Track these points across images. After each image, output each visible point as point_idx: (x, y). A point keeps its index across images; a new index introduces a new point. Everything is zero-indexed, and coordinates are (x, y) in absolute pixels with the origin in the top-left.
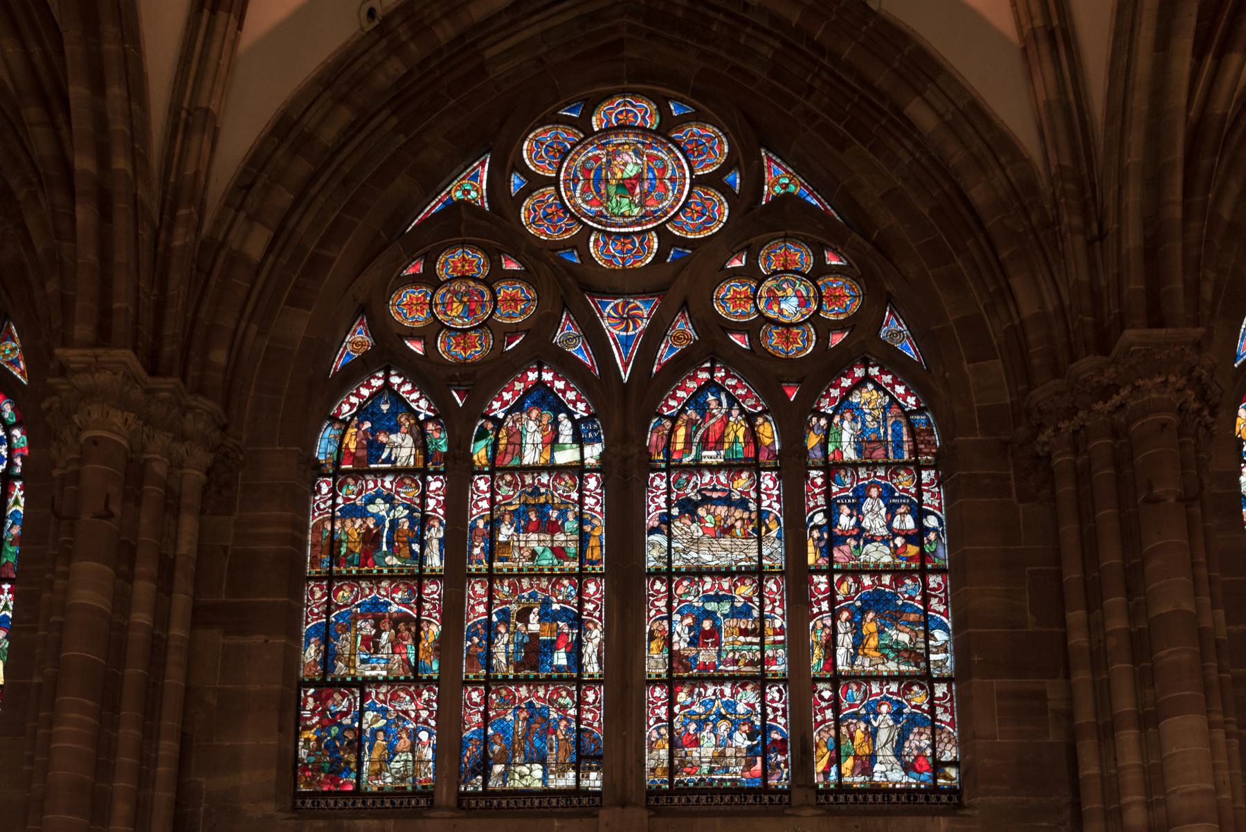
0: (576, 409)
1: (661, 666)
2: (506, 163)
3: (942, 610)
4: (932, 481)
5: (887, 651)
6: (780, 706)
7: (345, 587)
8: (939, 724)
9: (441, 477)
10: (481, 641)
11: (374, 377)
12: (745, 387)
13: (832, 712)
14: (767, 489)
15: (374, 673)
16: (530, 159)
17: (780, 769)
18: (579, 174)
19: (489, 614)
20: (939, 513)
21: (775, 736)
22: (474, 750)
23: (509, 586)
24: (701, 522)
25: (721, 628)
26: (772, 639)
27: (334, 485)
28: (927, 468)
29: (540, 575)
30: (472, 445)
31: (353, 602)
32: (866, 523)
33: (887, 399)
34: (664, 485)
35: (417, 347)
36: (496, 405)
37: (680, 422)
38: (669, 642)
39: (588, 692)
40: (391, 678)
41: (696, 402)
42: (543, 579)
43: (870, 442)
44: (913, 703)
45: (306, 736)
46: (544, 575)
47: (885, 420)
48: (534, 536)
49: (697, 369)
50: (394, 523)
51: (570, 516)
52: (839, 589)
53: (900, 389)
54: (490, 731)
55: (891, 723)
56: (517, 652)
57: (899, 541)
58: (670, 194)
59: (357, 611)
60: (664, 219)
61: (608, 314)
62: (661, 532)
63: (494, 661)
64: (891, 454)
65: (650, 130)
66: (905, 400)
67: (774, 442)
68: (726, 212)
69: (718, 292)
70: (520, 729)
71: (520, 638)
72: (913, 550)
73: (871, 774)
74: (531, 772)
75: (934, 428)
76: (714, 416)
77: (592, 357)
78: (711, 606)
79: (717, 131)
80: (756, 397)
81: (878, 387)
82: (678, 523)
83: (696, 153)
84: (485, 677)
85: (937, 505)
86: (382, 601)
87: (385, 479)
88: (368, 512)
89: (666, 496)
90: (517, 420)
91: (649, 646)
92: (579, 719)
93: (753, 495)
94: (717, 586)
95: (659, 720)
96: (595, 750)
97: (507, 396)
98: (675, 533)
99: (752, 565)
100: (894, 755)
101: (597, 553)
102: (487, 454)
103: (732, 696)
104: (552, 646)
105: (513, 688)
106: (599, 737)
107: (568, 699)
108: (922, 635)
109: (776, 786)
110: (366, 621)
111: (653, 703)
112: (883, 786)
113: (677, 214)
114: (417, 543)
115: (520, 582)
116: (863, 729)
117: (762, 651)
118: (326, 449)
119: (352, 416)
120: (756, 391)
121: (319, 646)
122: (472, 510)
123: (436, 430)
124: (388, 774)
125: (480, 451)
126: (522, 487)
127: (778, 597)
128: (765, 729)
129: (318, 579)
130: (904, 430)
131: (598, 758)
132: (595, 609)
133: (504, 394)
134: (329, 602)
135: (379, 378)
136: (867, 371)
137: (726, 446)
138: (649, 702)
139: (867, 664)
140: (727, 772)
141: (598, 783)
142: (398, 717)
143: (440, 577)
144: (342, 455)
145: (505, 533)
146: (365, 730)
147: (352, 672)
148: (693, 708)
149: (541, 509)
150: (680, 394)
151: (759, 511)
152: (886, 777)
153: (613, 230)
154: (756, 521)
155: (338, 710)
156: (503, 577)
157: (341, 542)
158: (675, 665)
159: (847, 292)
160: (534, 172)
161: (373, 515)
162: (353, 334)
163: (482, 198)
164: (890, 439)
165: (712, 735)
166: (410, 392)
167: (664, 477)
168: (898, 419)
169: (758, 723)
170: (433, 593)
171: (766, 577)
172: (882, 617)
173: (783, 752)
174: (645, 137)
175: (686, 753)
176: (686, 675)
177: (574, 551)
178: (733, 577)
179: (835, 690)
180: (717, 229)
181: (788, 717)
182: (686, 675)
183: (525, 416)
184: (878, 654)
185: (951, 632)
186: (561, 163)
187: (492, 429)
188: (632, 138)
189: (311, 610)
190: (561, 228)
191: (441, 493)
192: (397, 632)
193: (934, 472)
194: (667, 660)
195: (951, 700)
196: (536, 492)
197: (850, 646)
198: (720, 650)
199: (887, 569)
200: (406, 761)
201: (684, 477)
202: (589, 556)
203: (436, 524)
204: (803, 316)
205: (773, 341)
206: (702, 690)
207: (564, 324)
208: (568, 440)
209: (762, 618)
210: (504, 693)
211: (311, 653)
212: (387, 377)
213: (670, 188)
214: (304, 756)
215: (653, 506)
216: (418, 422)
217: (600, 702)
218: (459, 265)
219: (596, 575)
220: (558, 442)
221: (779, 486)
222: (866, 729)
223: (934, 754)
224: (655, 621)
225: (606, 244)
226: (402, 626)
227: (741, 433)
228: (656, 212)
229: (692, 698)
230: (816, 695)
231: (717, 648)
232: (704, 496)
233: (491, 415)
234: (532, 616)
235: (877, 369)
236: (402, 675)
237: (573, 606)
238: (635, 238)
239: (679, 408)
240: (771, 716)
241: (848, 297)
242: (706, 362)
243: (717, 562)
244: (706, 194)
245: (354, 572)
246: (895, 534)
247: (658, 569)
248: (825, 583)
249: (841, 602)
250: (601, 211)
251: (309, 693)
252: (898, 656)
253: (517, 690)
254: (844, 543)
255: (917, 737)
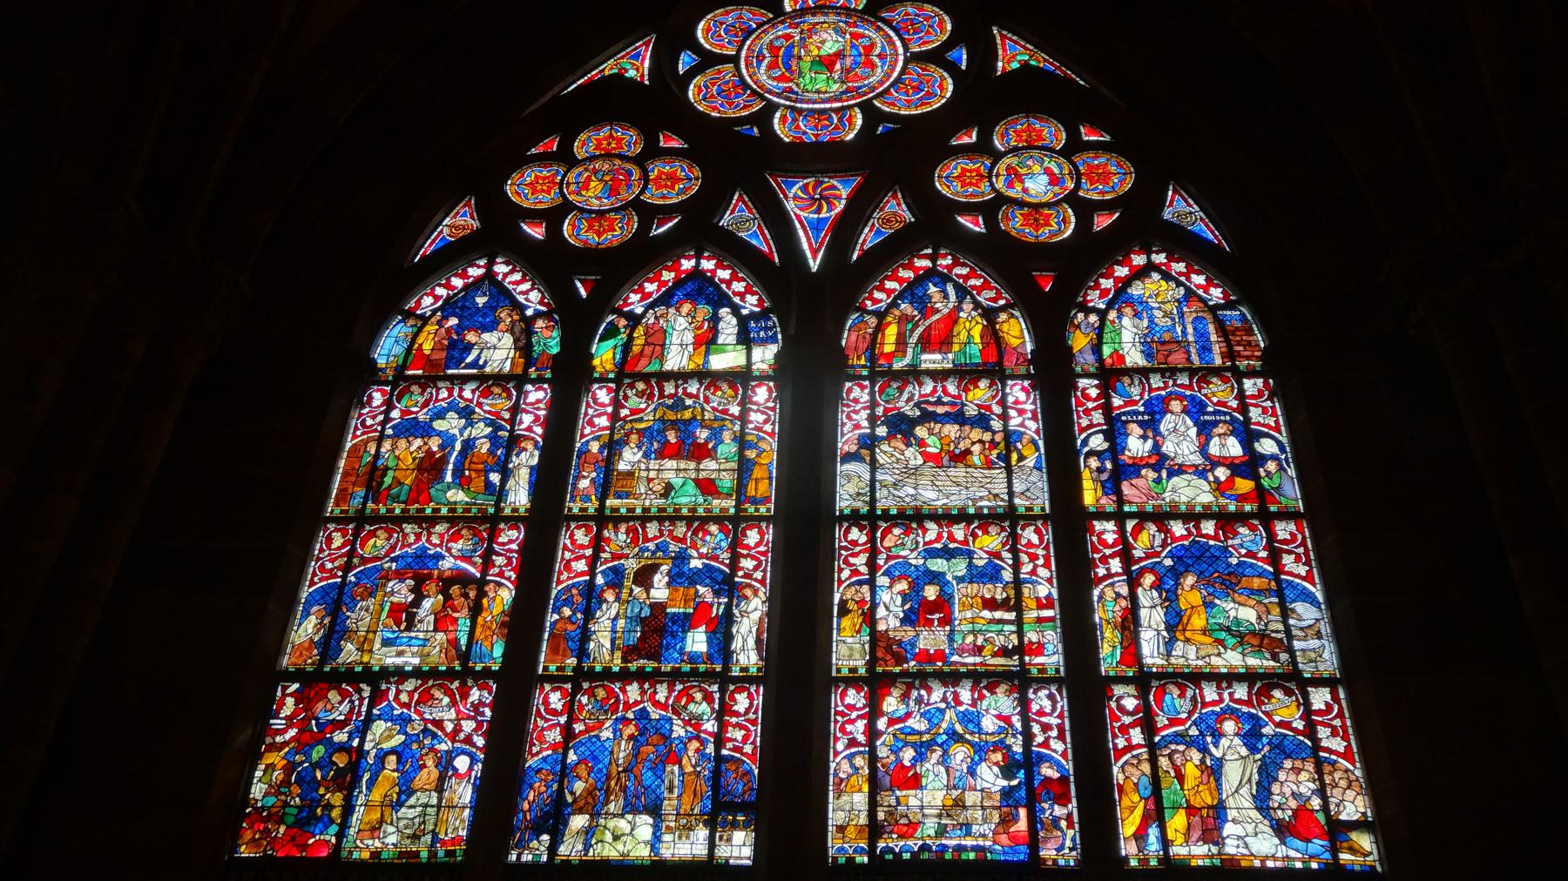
0: (745, 302)
1: (857, 656)
2: (677, 38)
3: (1303, 574)
4: (1260, 394)
5: (1223, 635)
6: (1054, 721)
7: (379, 533)
8: (1327, 755)
9: (546, 386)
10: (574, 614)
11: (473, 265)
12: (980, 277)
13: (1142, 733)
14: (1017, 402)
15: (399, 661)
16: (705, 38)
17: (1060, 829)
18: (765, 52)
19: (592, 572)
20: (1277, 435)
21: (1048, 771)
22: (543, 789)
23: (627, 533)
24: (920, 446)
25: (953, 597)
26: (1036, 615)
27: (391, 394)
28: (1252, 374)
29: (673, 519)
30: (595, 346)
31: (387, 554)
32: (1168, 448)
33: (1182, 291)
34: (865, 397)
35: (536, 232)
36: (634, 298)
37: (889, 319)
38: (870, 618)
39: (737, 696)
40: (426, 668)
41: (913, 295)
42: (679, 524)
43: (1163, 343)
44: (1277, 719)
45: (270, 762)
46: (682, 518)
47: (1182, 315)
48: (670, 464)
49: (914, 256)
50: (468, 445)
51: (727, 436)
52: (1135, 540)
53: (1199, 279)
54: (572, 757)
55: (1244, 751)
56: (629, 631)
57: (1222, 473)
58: (879, 70)
59: (390, 567)
60: (871, 95)
61: (793, 197)
62: (860, 459)
63: (592, 645)
64: (1195, 358)
65: (855, 10)
66: (1206, 291)
67: (1024, 343)
68: (951, 88)
69: (941, 170)
70: (622, 755)
71: (636, 610)
72: (1244, 485)
73: (1219, 841)
74: (632, 830)
75: (1254, 326)
76: (938, 311)
77: (771, 242)
78: (937, 565)
79: (938, 10)
80: (997, 289)
81: (1167, 276)
82: (885, 447)
83: (911, 31)
84: (574, 670)
85: (1273, 425)
86: (432, 552)
87: (464, 387)
88: (434, 430)
89: (868, 412)
90: (662, 316)
91: (839, 625)
92: (720, 740)
93: (997, 409)
94: (945, 535)
95: (853, 742)
96: (744, 793)
97: (650, 287)
98: (881, 461)
99: (1000, 506)
100: (1256, 808)
101: (763, 488)
102: (614, 358)
103: (974, 704)
104: (688, 622)
105: (616, 687)
106: (750, 772)
107: (704, 705)
108: (1276, 611)
109: (1055, 861)
110: (402, 581)
111: (843, 714)
112: (1244, 864)
113: (888, 88)
114: (497, 471)
115: (644, 528)
116: (1198, 763)
117: (1020, 633)
118: (390, 350)
119: (434, 312)
120: (996, 282)
121: (322, 619)
122: (583, 428)
123: (546, 327)
124: (391, 829)
125: (604, 354)
126: (659, 399)
127: (1040, 552)
128: (1030, 761)
129: (342, 521)
130: (1211, 328)
131: (743, 807)
132: (756, 568)
133: (647, 285)
134: (351, 554)
135: (479, 267)
136: (1149, 258)
137: (956, 348)
138: (837, 713)
139: (1192, 655)
140: (968, 834)
141: (747, 852)
142: (425, 731)
143: (520, 519)
144: (410, 359)
145: (629, 457)
146: (368, 752)
147: (366, 659)
148: (910, 722)
149: (684, 427)
150: (889, 285)
151: (1008, 434)
152: (1247, 846)
153: (805, 106)
154: (1002, 445)
155: (331, 718)
156: (616, 520)
157: (387, 469)
158: (879, 654)
159: (1113, 169)
160: (711, 51)
161: (439, 434)
162: (455, 217)
163: (642, 76)
164: (1191, 338)
165: (942, 769)
166: (517, 283)
167: (865, 387)
168: (1200, 314)
169: (1018, 749)
170: (510, 542)
171: (1022, 523)
172: (1209, 584)
173: (1063, 800)
174: (848, 15)
175: (897, 799)
176: (897, 670)
177: (729, 485)
178: (969, 523)
179: (1143, 695)
180: (939, 105)
181: (1068, 739)
182: (897, 670)
183: (672, 310)
184: (1208, 640)
185: (1323, 607)
186: (743, 42)
187: (625, 327)
188: (832, 18)
189: (323, 565)
190: (739, 104)
191: (542, 406)
192: (448, 598)
193: (1262, 380)
194: (867, 646)
195: (1340, 715)
196: (678, 405)
197: (1162, 627)
198: (952, 631)
199: (1207, 514)
200: (426, 806)
201: (895, 386)
202: (751, 491)
203: (530, 447)
204: (1055, 195)
205: (1015, 223)
206: (923, 692)
207: (736, 206)
208: (732, 339)
209: (1018, 583)
210: (601, 693)
211: (306, 629)
212: (489, 266)
213: (879, 64)
214: (258, 796)
215: (849, 426)
216: (524, 318)
217: (756, 712)
218: (605, 142)
219: (761, 518)
220: (715, 343)
221: (1035, 399)
222: (1203, 761)
223: (1325, 808)
224: (849, 586)
225: (795, 120)
226: (455, 590)
227: (977, 332)
228: (860, 88)
229: (908, 706)
230: (1113, 704)
231: (948, 628)
232: (924, 411)
233: (626, 309)
234: (657, 577)
235: (1164, 255)
236: (443, 664)
237: (722, 563)
238: (833, 114)
239: (889, 301)
240: (1040, 739)
241: (1115, 174)
242: (927, 248)
243: (945, 501)
244: (923, 70)
245: (397, 511)
246: (1215, 462)
247: (855, 512)
248: (1114, 532)
249: (1141, 559)
250: (790, 88)
251: (288, 691)
252: (1241, 643)
253: (624, 691)
254: (1139, 476)
255: (1292, 777)
